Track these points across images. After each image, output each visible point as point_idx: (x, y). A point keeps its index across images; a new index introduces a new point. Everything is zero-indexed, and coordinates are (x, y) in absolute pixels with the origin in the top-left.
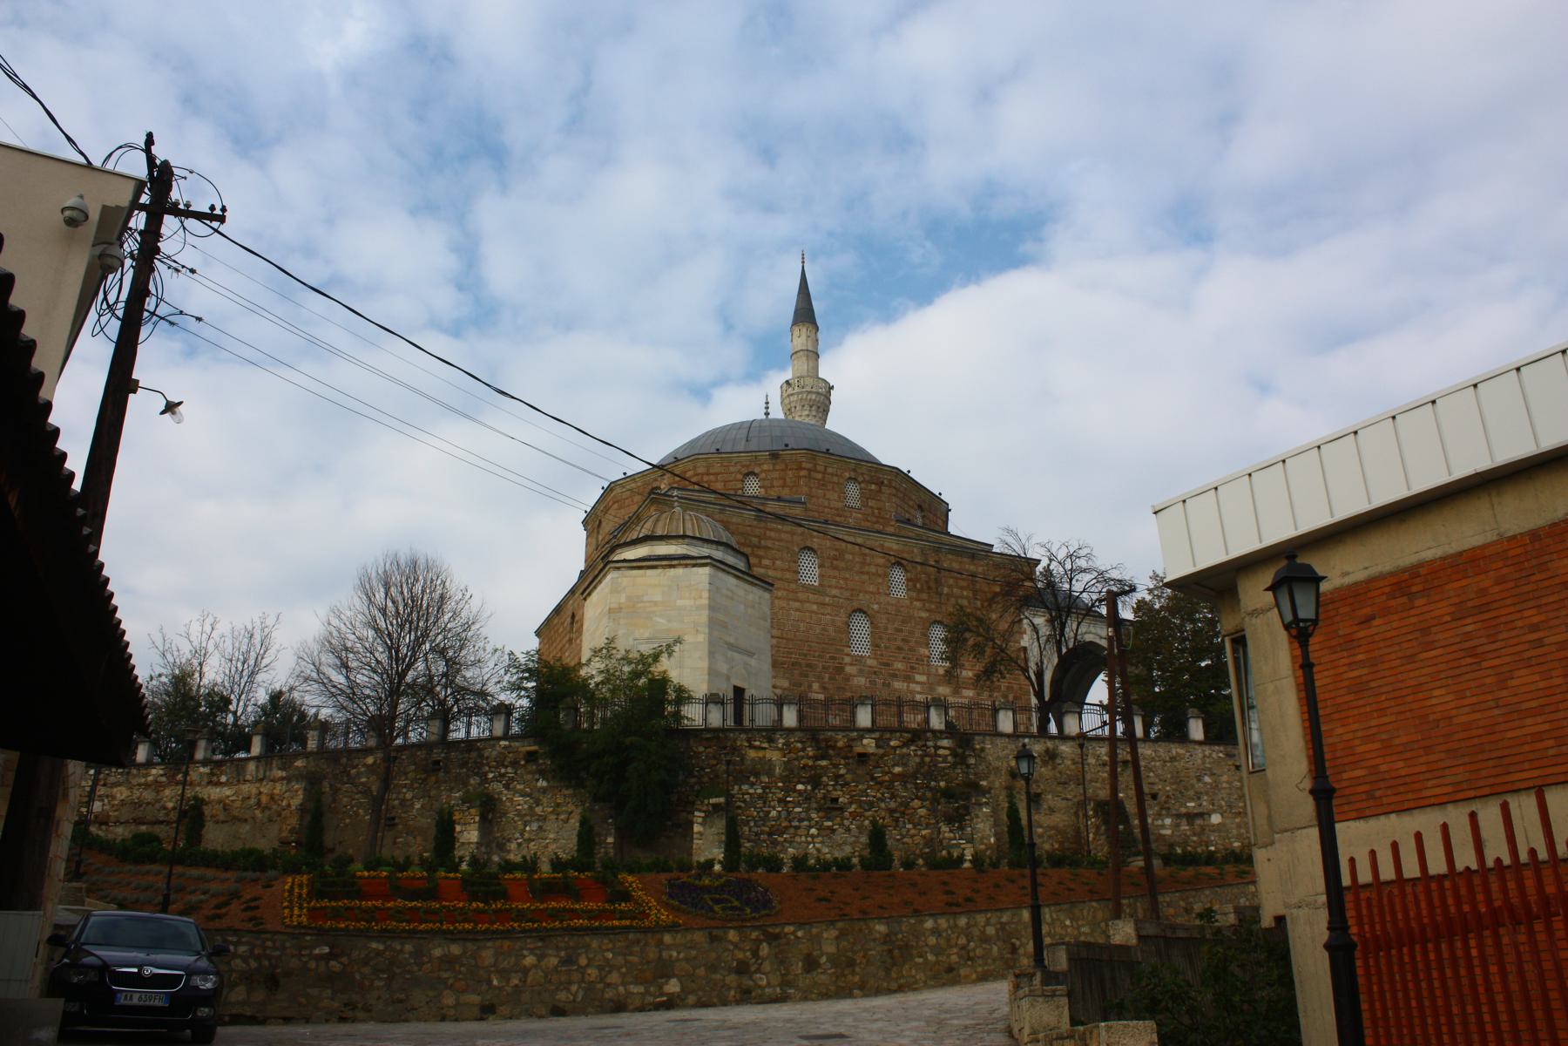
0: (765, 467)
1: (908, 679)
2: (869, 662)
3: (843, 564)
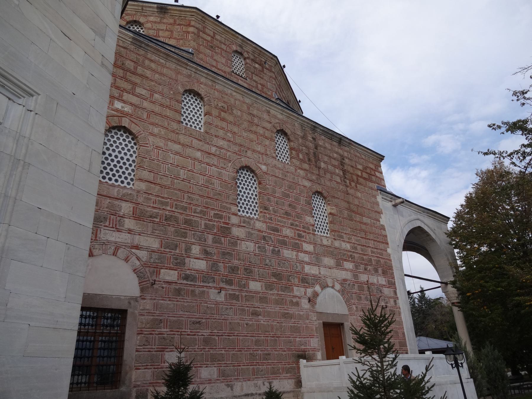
0: (152, 19)
1: (297, 248)
2: (259, 225)
3: (231, 118)
